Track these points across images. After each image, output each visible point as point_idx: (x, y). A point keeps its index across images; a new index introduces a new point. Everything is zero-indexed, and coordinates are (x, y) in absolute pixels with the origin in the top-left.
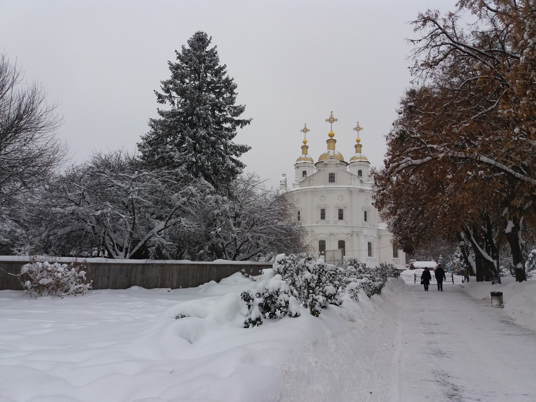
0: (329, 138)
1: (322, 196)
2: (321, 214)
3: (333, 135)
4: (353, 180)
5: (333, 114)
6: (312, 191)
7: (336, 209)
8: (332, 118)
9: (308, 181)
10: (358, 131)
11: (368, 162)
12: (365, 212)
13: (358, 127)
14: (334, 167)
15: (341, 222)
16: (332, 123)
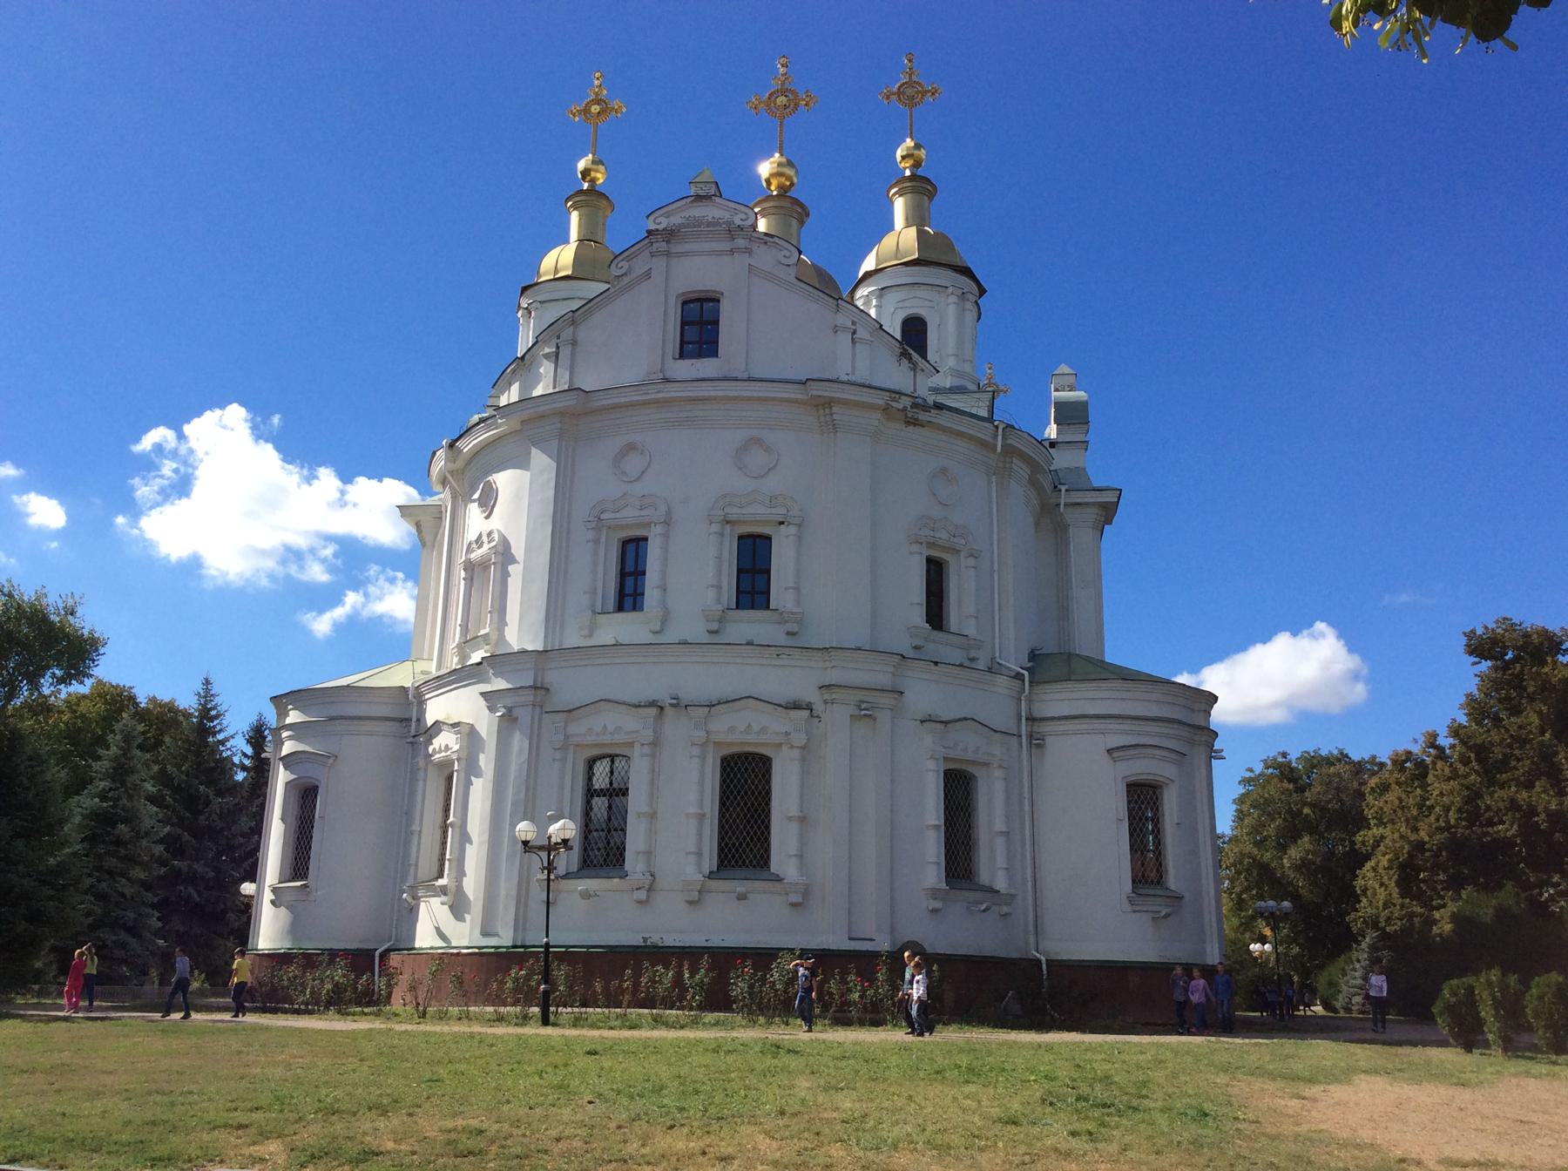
1: (631, 447)
6: (561, 414)
11: (967, 272)
13: (911, 84)
14: (719, 253)
15: (750, 625)
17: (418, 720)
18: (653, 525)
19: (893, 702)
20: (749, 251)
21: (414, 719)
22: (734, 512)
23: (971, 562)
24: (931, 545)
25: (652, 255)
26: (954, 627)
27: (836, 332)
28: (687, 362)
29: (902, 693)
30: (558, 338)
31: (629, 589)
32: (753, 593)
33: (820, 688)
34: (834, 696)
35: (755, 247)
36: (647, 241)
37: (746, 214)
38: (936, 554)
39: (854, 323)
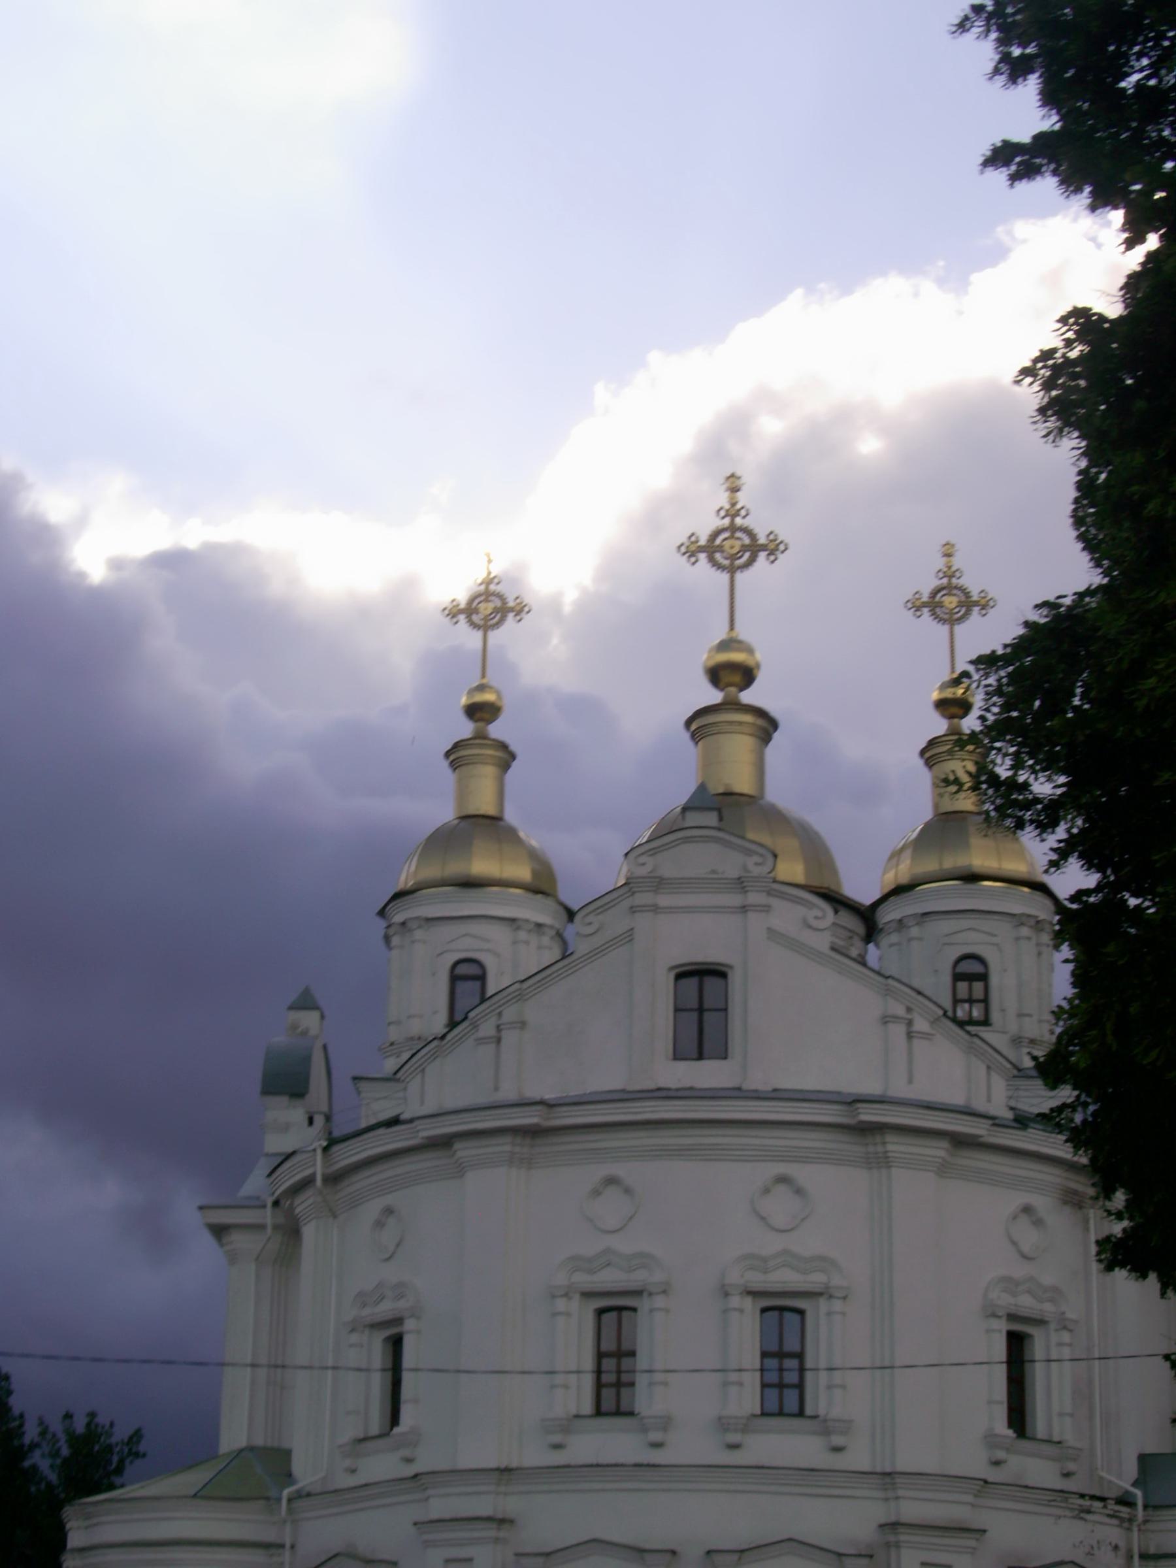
0: (715, 696)
1: (611, 1181)
2: (600, 1356)
3: (747, 675)
4: (899, 1030)
5: (743, 499)
7: (735, 1301)
8: (733, 528)
9: (480, 1041)
10: (951, 620)
12: (1017, 1343)
13: (949, 589)
16: (732, 570)
17: (293, 1547)
18: (645, 1294)
19: (973, 1543)
20: (767, 909)
21: (288, 1545)
22: (757, 1280)
23: (1066, 1337)
24: (1012, 1317)
25: (633, 910)
26: (1040, 1429)
27: (886, 1023)
28: (682, 1065)
29: (985, 1531)
30: (500, 1014)
31: (607, 1378)
32: (781, 1386)
33: (881, 1526)
34: (902, 1538)
35: (775, 902)
36: (626, 889)
37: (761, 855)
38: (1017, 1327)
39: (909, 1010)
